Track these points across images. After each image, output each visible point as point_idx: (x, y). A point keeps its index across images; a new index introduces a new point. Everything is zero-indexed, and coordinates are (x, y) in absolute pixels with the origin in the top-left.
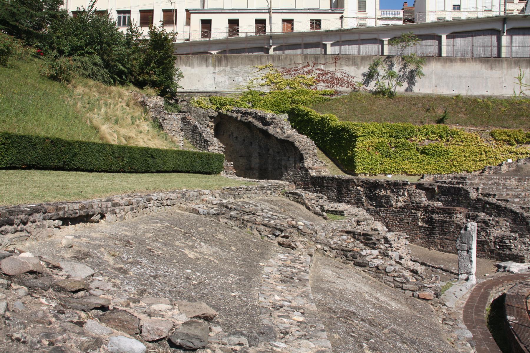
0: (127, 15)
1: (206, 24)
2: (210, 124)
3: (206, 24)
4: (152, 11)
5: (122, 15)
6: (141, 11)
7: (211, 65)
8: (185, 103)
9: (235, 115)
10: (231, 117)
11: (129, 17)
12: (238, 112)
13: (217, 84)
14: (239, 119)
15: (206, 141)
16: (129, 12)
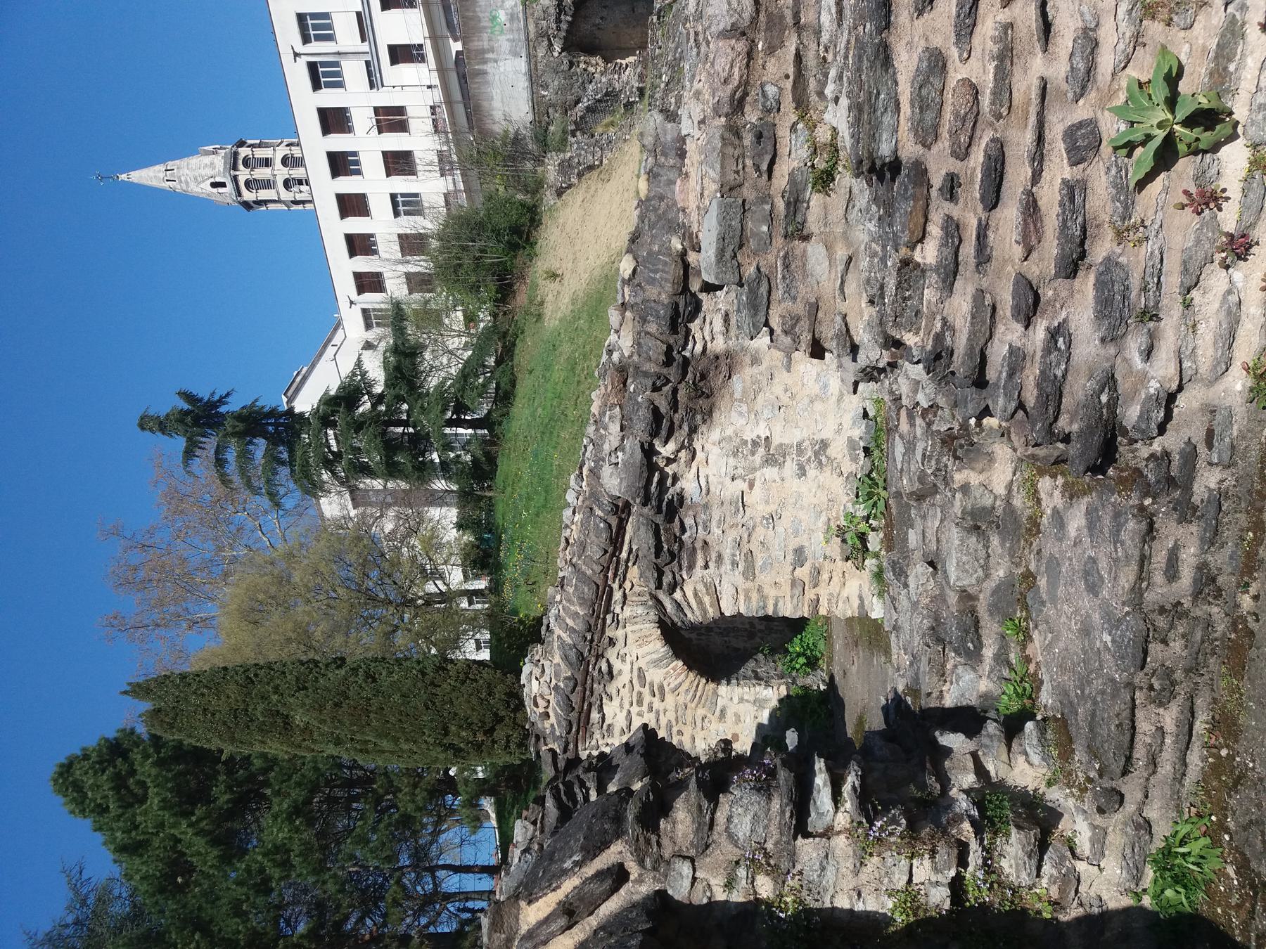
0: (400, 199)
1: (401, 54)
2: (582, 66)
3: (401, 54)
4: (385, 154)
5: (401, 208)
6: (388, 175)
7: (485, 67)
8: (550, 110)
9: (564, 26)
10: (567, 31)
11: (403, 195)
12: (558, 21)
13: (516, 54)
14: (569, 19)
15: (607, 94)
16: (393, 197)
